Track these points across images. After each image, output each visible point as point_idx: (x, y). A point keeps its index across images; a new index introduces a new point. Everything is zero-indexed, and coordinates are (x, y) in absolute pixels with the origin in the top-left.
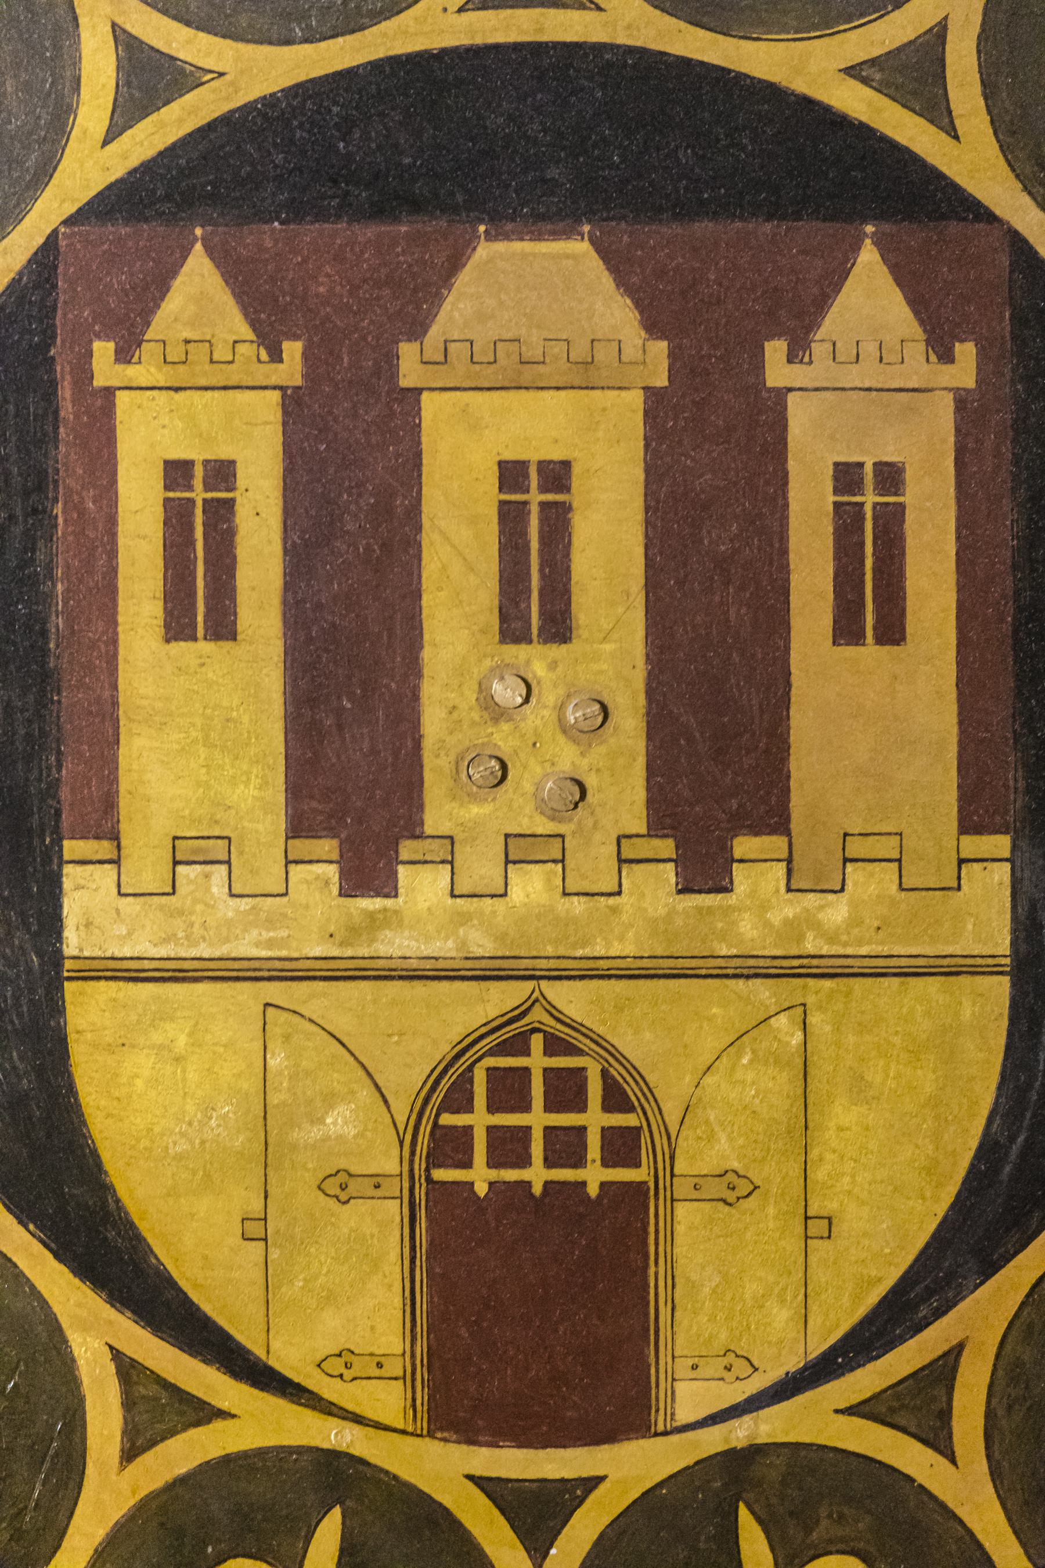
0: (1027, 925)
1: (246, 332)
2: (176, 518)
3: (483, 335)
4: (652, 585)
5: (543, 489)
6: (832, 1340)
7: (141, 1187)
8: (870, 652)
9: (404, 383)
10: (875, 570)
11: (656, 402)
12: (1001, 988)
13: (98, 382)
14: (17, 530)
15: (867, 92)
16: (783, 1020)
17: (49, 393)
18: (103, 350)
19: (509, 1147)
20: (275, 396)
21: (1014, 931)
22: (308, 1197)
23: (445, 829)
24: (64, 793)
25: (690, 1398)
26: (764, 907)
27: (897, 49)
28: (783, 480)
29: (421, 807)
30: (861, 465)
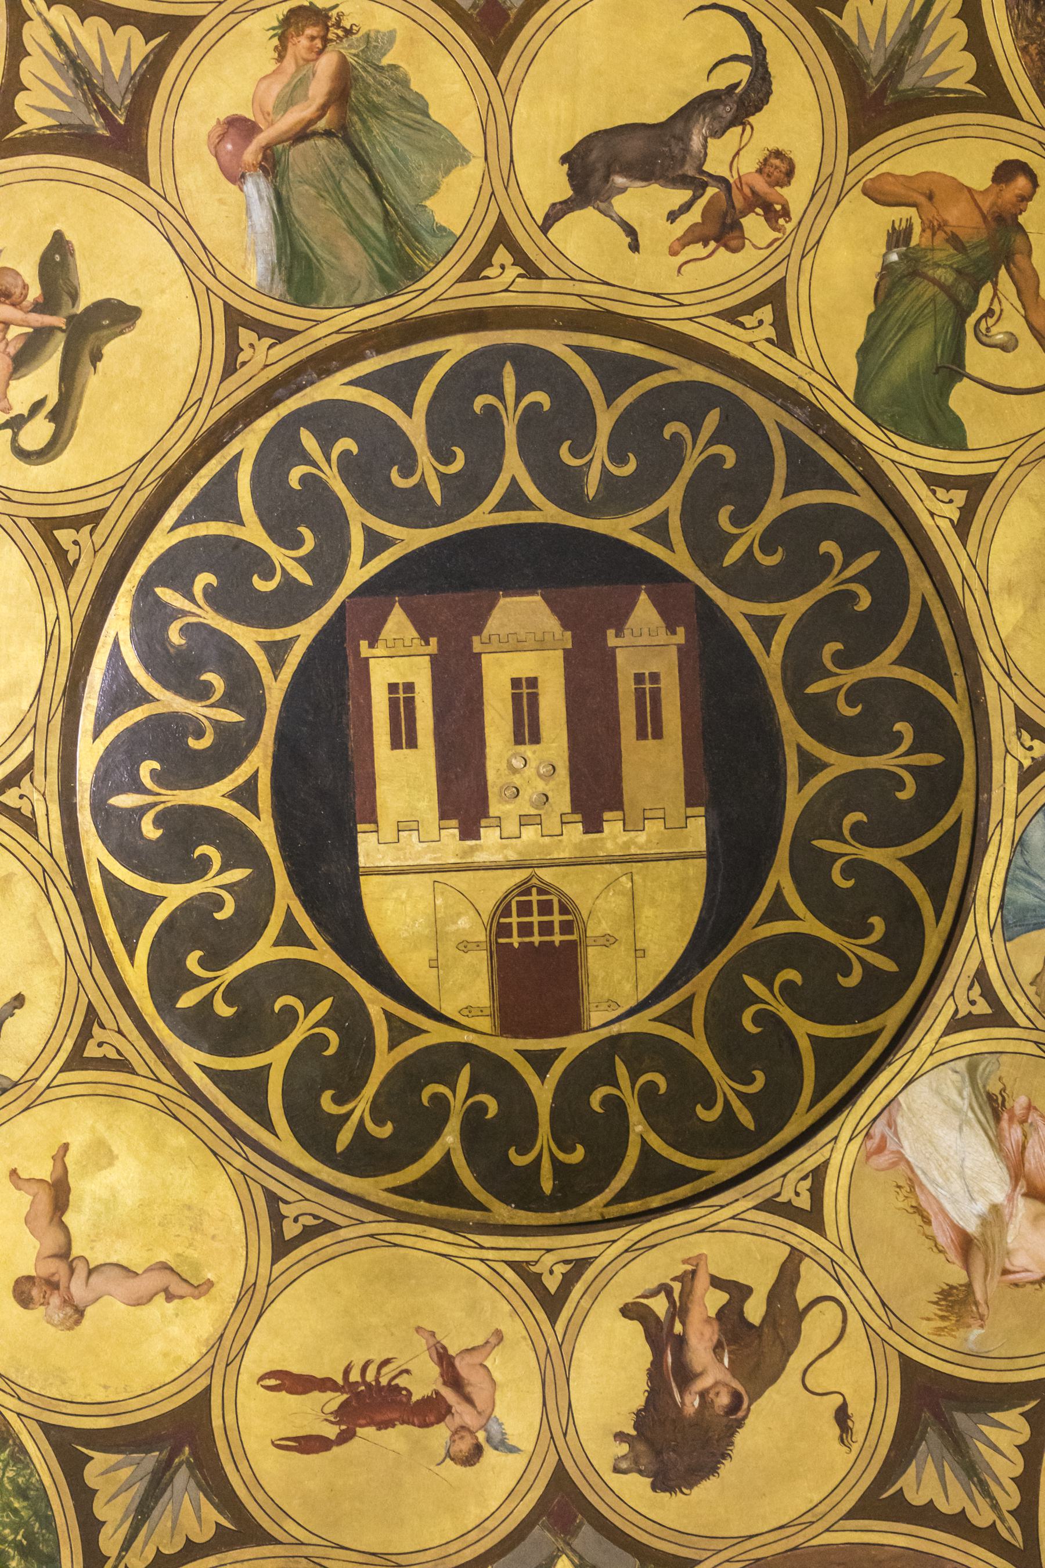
0: (710, 840)
1: (415, 634)
2: (393, 704)
3: (503, 632)
5: (527, 688)
6: (647, 994)
8: (650, 743)
9: (475, 651)
12: (703, 862)
13: (363, 655)
16: (624, 879)
17: (345, 661)
18: (364, 644)
19: (525, 929)
20: (428, 658)
22: (452, 951)
25: (596, 1018)
26: (615, 837)
28: (615, 680)
29: (488, 807)
30: (644, 674)
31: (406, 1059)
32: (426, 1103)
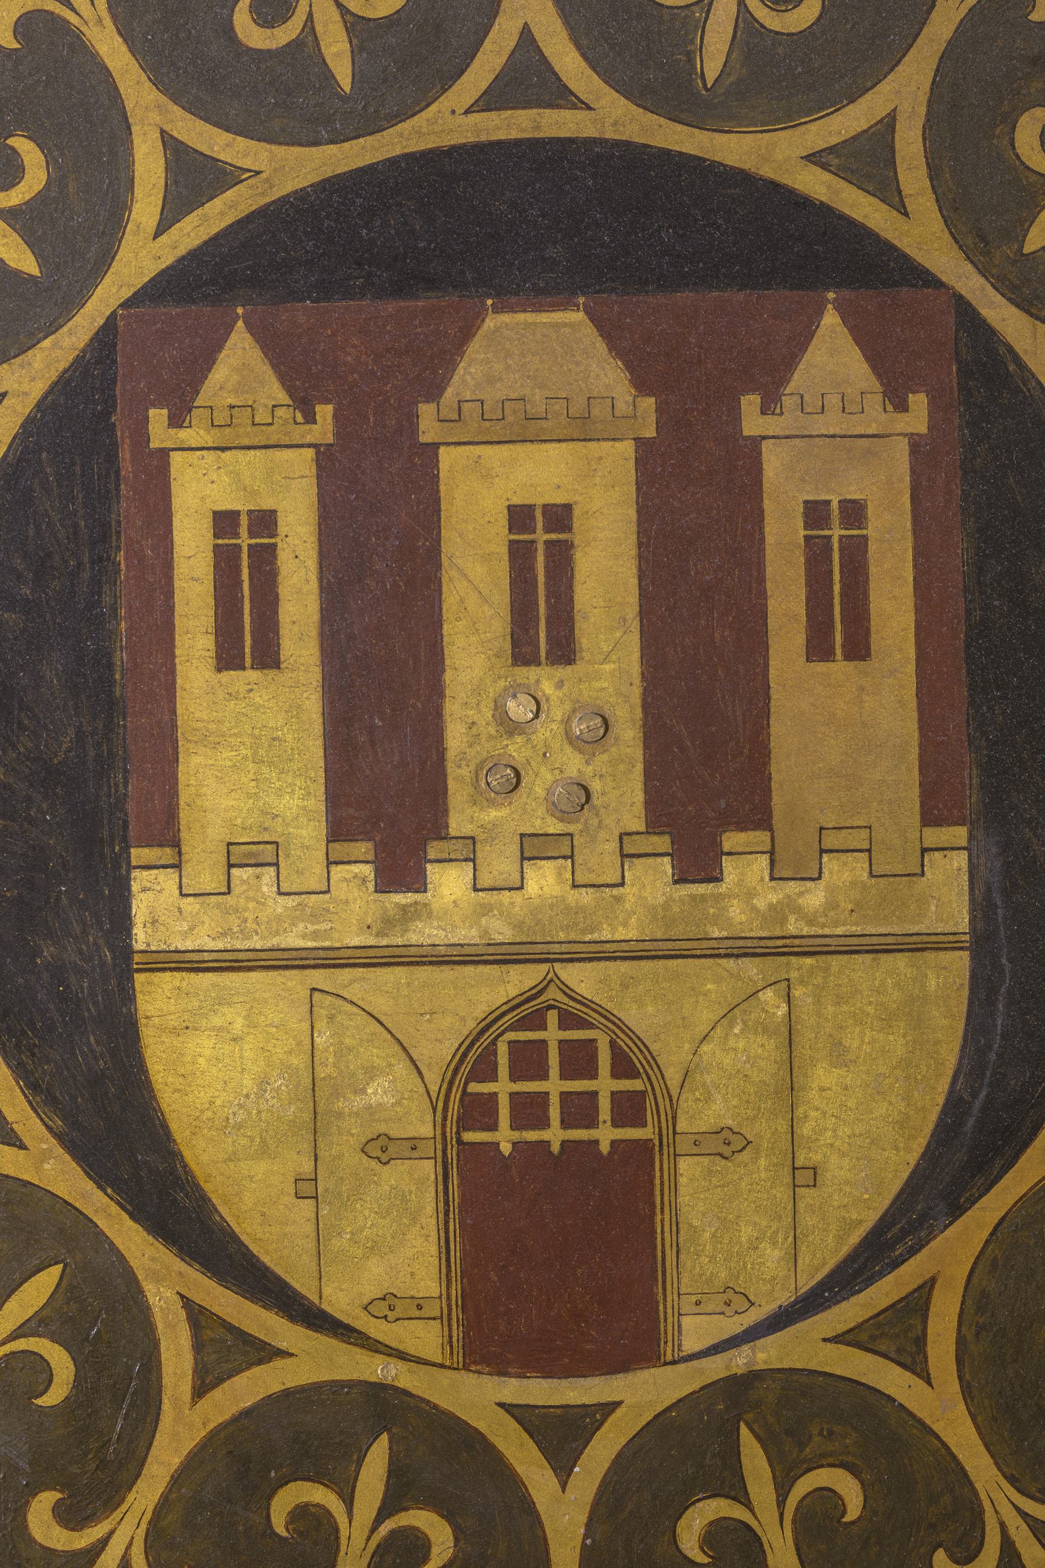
0: (981, 907)
2: (225, 562)
3: (492, 395)
4: (644, 613)
5: (547, 530)
6: (819, 1277)
7: (202, 1153)
8: (839, 668)
9: (422, 439)
10: (842, 595)
11: (646, 453)
12: (961, 961)
14: (86, 575)
15: (826, 176)
16: (768, 995)
18: (158, 417)
19: (529, 1111)
20: (310, 453)
21: (972, 911)
22: (353, 1159)
23: (468, 830)
24: (131, 807)
25: (695, 1331)
26: (751, 894)
27: (853, 138)
29: (446, 812)
30: (828, 503)
31: (235, 1419)
32: (281, 1530)
